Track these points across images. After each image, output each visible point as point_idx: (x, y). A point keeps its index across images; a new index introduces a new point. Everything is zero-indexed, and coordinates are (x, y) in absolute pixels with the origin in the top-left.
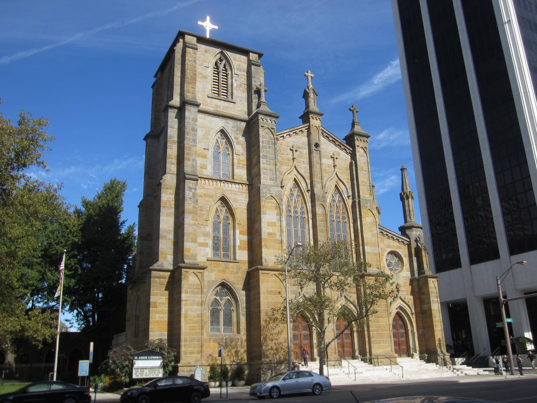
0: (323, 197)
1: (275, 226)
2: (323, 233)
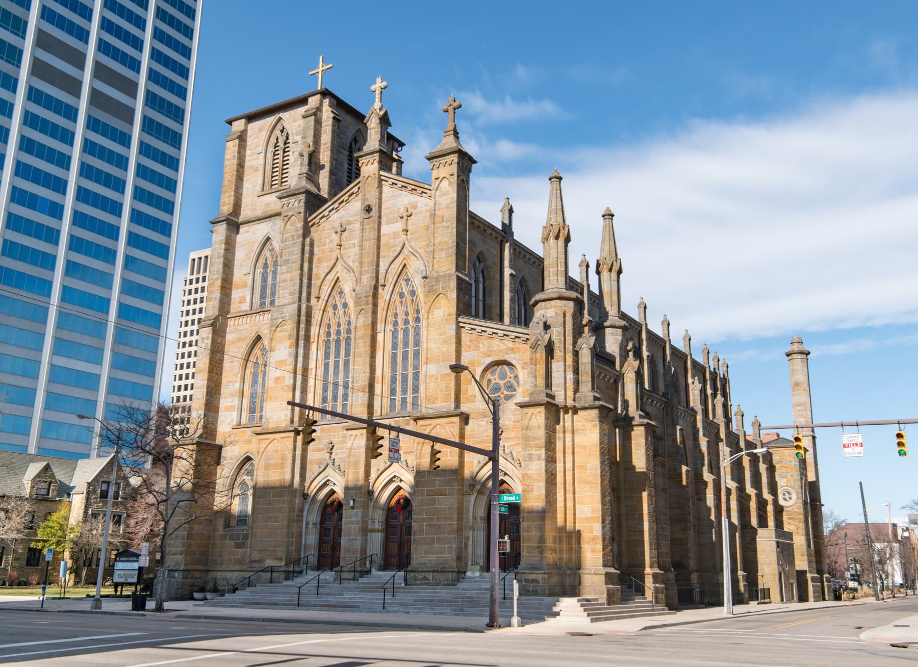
0: (365, 297)
2: (361, 357)
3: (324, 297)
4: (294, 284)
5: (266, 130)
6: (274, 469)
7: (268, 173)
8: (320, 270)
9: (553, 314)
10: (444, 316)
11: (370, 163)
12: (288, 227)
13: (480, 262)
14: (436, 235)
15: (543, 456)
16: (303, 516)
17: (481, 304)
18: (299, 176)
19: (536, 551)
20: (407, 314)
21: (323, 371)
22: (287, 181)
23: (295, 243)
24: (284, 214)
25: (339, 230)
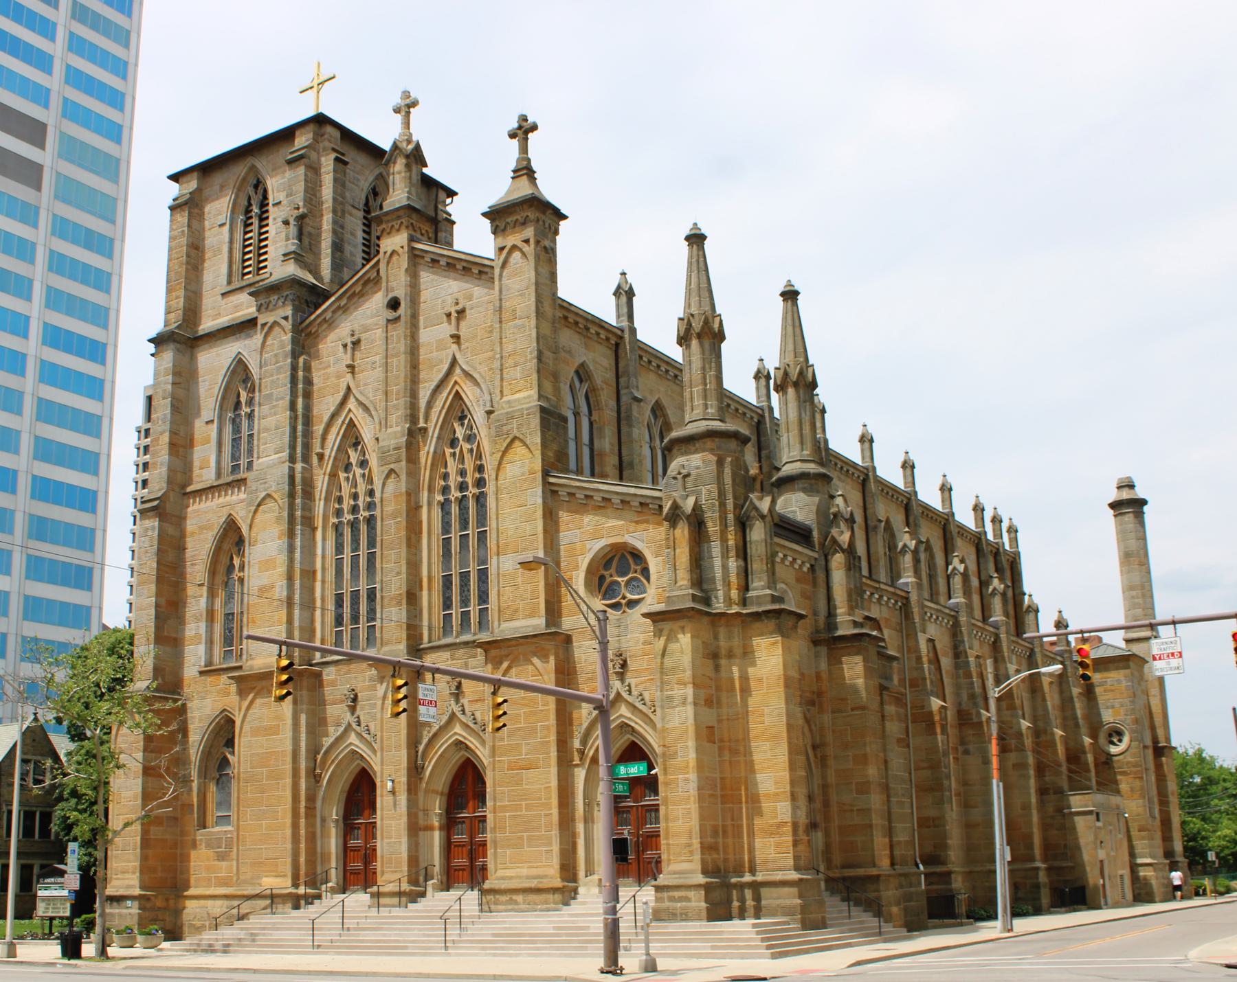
0: (396, 449)
1: (274, 567)
3: (330, 450)
4: (283, 433)
5: (232, 186)
6: (264, 736)
7: (237, 255)
8: (324, 407)
9: (700, 463)
10: (523, 474)
11: (394, 231)
12: (269, 342)
13: (581, 381)
14: (504, 340)
15: (690, 699)
16: (315, 808)
17: (586, 451)
18: (283, 258)
19: (685, 851)
20: (463, 473)
21: (334, 573)
22: (265, 267)
23: (281, 367)
24: (260, 322)
25: (349, 340)
